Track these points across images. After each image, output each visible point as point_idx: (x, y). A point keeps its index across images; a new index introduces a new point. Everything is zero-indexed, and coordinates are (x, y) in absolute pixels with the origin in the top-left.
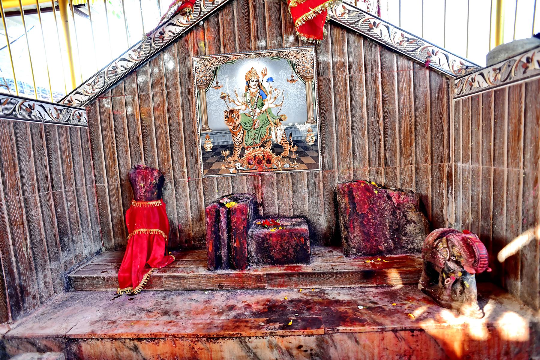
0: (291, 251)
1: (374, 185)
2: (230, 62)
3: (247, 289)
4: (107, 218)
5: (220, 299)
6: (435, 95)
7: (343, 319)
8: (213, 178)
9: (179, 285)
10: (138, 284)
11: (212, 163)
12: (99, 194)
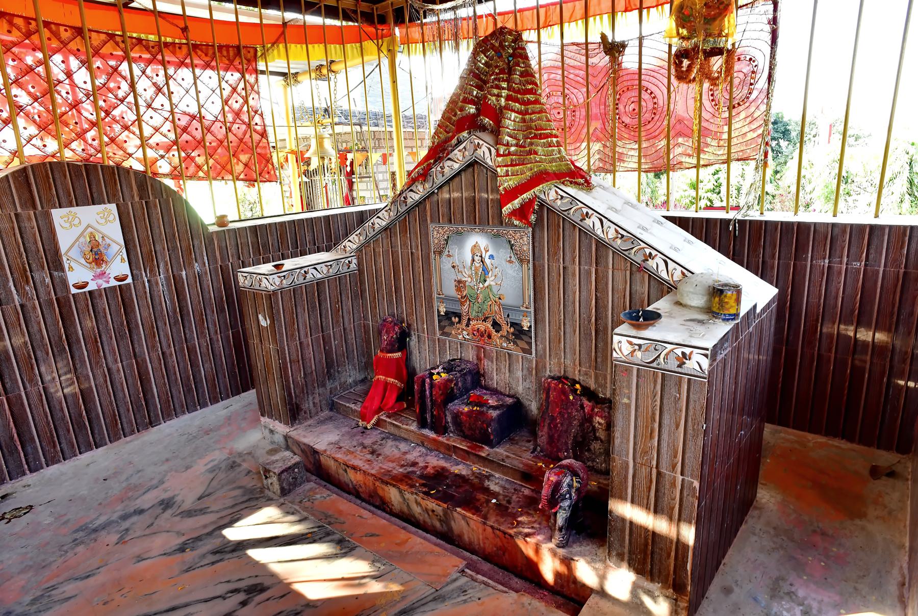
2: (459, 233)
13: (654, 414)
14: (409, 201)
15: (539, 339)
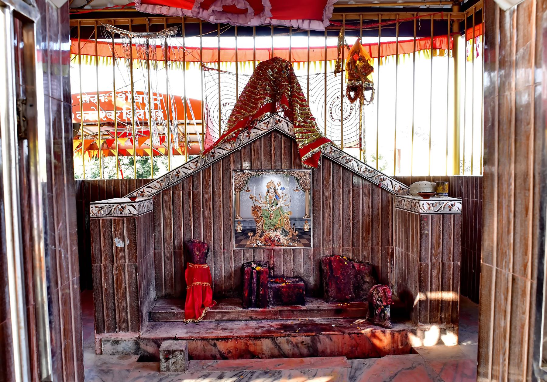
0: (294, 297)
1: (345, 259)
3: (268, 319)
4: (161, 275)
5: (253, 324)
6: (385, 204)
7: (325, 330)
8: (241, 250)
9: (225, 317)
10: (200, 316)
11: (241, 240)
12: (157, 258)
13: (440, 235)
14: (217, 155)
15: (316, 235)
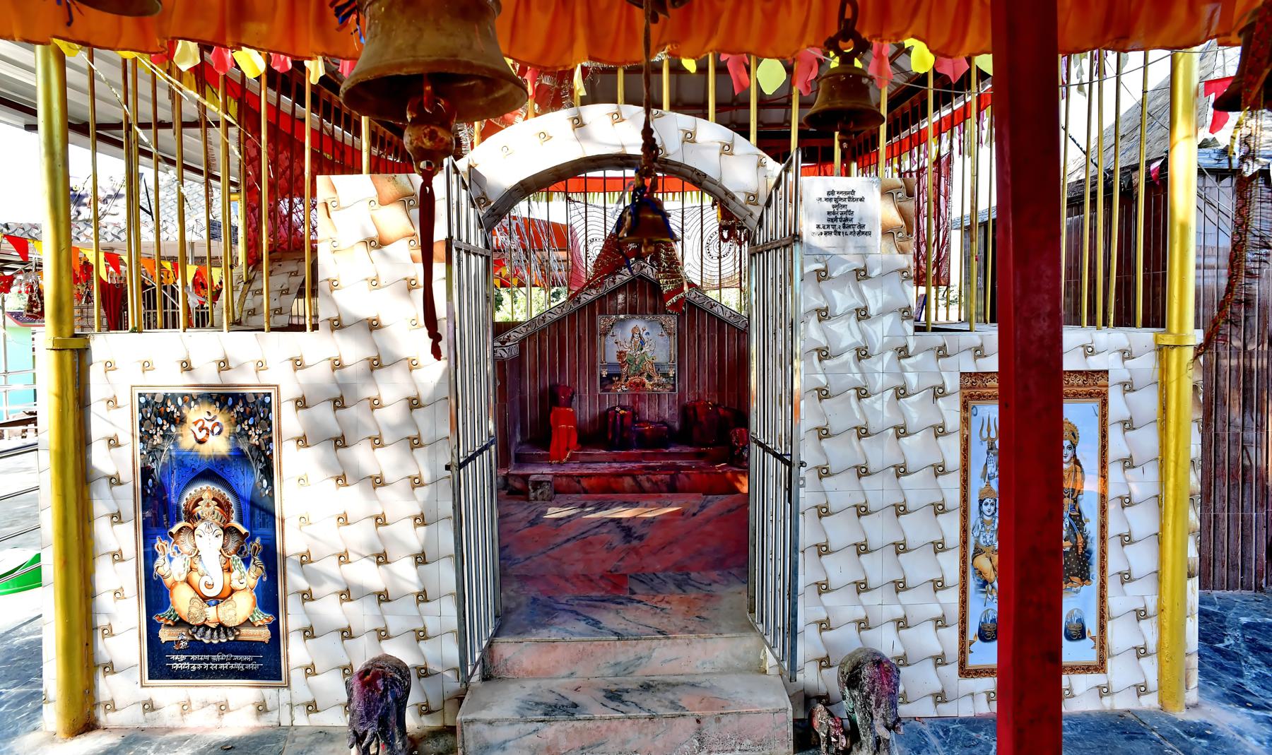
9: (588, 459)
14: (583, 301)
